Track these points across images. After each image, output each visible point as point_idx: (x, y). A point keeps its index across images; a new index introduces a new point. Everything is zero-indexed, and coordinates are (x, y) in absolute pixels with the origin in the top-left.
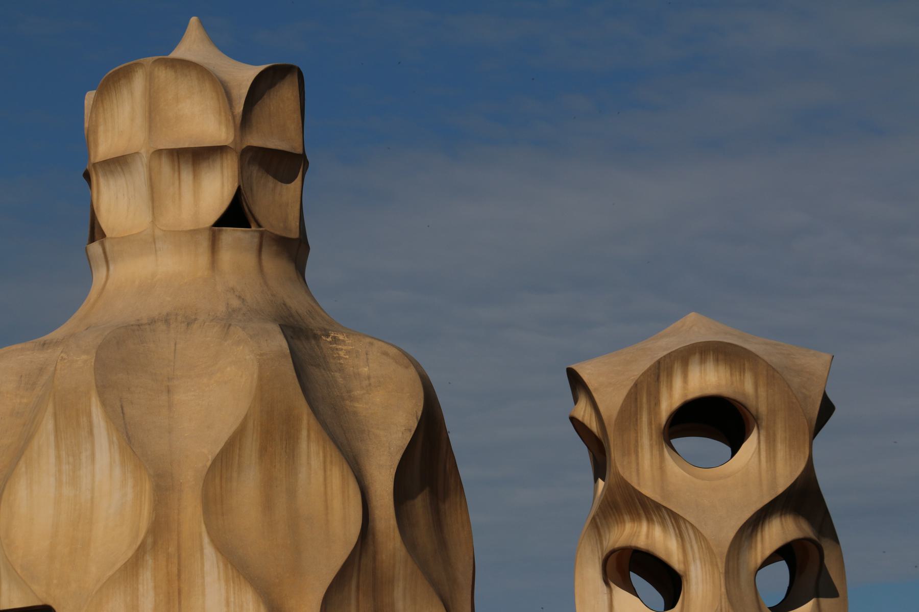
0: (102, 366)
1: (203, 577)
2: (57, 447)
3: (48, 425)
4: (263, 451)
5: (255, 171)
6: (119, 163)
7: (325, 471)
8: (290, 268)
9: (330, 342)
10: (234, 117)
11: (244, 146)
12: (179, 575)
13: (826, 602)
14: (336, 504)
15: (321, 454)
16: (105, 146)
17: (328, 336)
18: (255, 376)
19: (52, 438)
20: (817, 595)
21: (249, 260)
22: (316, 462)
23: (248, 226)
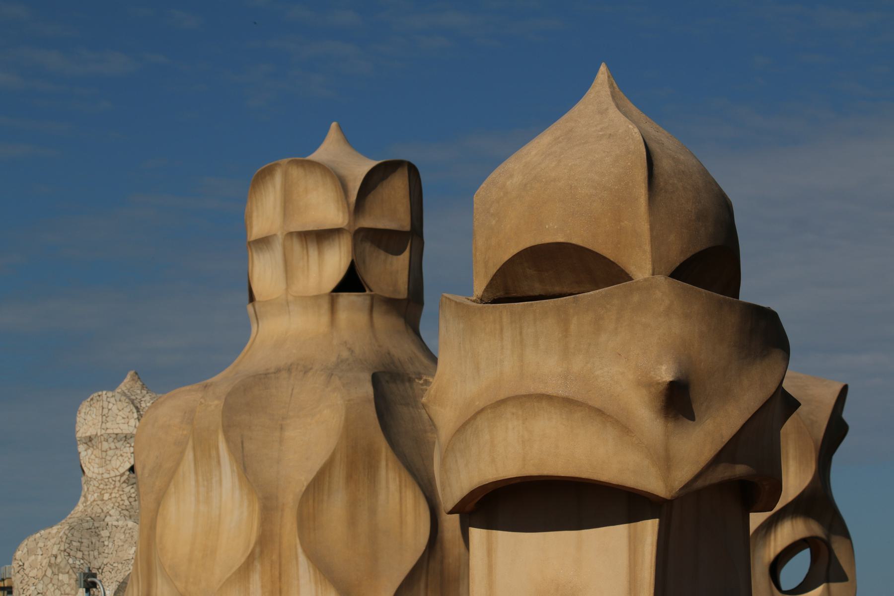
0: (229, 410)
1: (298, 580)
2: (196, 473)
3: (189, 455)
4: (349, 477)
5: (368, 247)
6: (264, 242)
7: (401, 493)
8: (399, 323)
9: (422, 385)
10: (348, 204)
11: (357, 228)
12: (280, 578)
13: (835, 587)
14: (410, 519)
15: (397, 479)
16: (257, 229)
17: (420, 379)
18: (343, 418)
19: (192, 465)
20: (828, 580)
21: (362, 318)
22: (393, 486)
23: (364, 291)
